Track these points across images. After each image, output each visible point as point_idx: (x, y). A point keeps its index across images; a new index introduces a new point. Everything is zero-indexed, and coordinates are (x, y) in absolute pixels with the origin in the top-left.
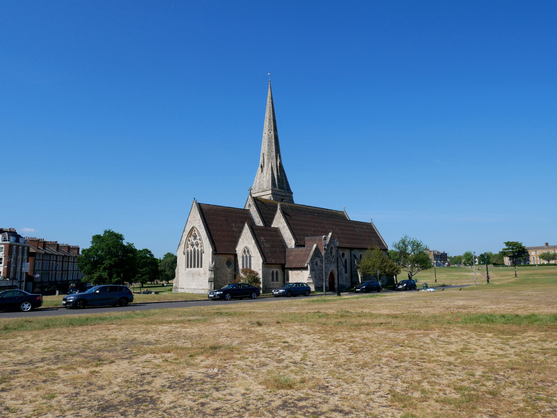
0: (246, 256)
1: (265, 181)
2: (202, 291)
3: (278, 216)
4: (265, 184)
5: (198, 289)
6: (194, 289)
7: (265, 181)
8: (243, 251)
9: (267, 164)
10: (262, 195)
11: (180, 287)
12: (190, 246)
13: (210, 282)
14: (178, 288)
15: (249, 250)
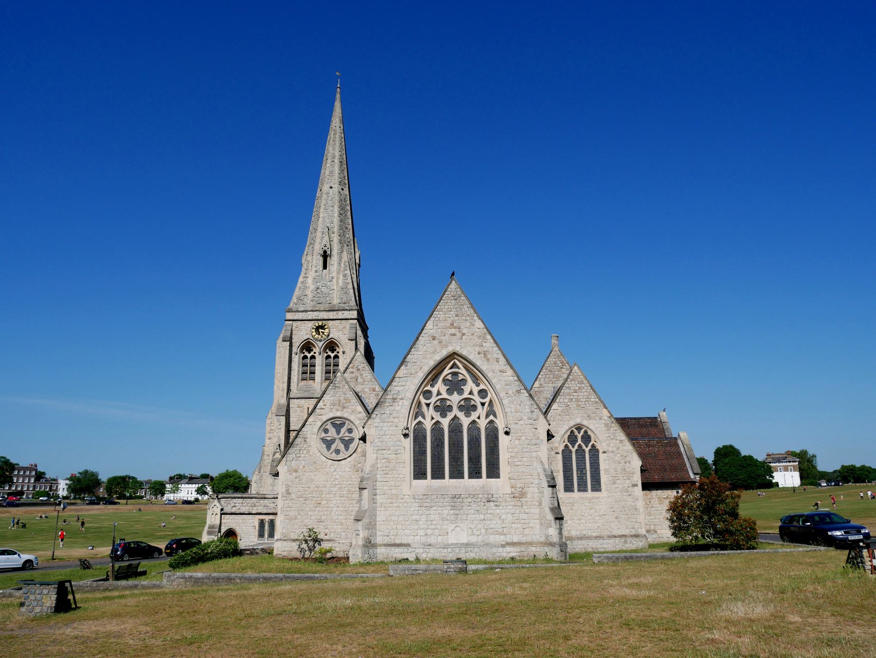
0: (580, 452)
1: (335, 287)
2: (508, 549)
4: (335, 295)
5: (487, 544)
6: (467, 545)
7: (335, 287)
8: (567, 436)
9: (338, 253)
10: (326, 318)
11: (379, 540)
12: (430, 412)
13: (558, 521)
14: (375, 546)
15: (590, 433)
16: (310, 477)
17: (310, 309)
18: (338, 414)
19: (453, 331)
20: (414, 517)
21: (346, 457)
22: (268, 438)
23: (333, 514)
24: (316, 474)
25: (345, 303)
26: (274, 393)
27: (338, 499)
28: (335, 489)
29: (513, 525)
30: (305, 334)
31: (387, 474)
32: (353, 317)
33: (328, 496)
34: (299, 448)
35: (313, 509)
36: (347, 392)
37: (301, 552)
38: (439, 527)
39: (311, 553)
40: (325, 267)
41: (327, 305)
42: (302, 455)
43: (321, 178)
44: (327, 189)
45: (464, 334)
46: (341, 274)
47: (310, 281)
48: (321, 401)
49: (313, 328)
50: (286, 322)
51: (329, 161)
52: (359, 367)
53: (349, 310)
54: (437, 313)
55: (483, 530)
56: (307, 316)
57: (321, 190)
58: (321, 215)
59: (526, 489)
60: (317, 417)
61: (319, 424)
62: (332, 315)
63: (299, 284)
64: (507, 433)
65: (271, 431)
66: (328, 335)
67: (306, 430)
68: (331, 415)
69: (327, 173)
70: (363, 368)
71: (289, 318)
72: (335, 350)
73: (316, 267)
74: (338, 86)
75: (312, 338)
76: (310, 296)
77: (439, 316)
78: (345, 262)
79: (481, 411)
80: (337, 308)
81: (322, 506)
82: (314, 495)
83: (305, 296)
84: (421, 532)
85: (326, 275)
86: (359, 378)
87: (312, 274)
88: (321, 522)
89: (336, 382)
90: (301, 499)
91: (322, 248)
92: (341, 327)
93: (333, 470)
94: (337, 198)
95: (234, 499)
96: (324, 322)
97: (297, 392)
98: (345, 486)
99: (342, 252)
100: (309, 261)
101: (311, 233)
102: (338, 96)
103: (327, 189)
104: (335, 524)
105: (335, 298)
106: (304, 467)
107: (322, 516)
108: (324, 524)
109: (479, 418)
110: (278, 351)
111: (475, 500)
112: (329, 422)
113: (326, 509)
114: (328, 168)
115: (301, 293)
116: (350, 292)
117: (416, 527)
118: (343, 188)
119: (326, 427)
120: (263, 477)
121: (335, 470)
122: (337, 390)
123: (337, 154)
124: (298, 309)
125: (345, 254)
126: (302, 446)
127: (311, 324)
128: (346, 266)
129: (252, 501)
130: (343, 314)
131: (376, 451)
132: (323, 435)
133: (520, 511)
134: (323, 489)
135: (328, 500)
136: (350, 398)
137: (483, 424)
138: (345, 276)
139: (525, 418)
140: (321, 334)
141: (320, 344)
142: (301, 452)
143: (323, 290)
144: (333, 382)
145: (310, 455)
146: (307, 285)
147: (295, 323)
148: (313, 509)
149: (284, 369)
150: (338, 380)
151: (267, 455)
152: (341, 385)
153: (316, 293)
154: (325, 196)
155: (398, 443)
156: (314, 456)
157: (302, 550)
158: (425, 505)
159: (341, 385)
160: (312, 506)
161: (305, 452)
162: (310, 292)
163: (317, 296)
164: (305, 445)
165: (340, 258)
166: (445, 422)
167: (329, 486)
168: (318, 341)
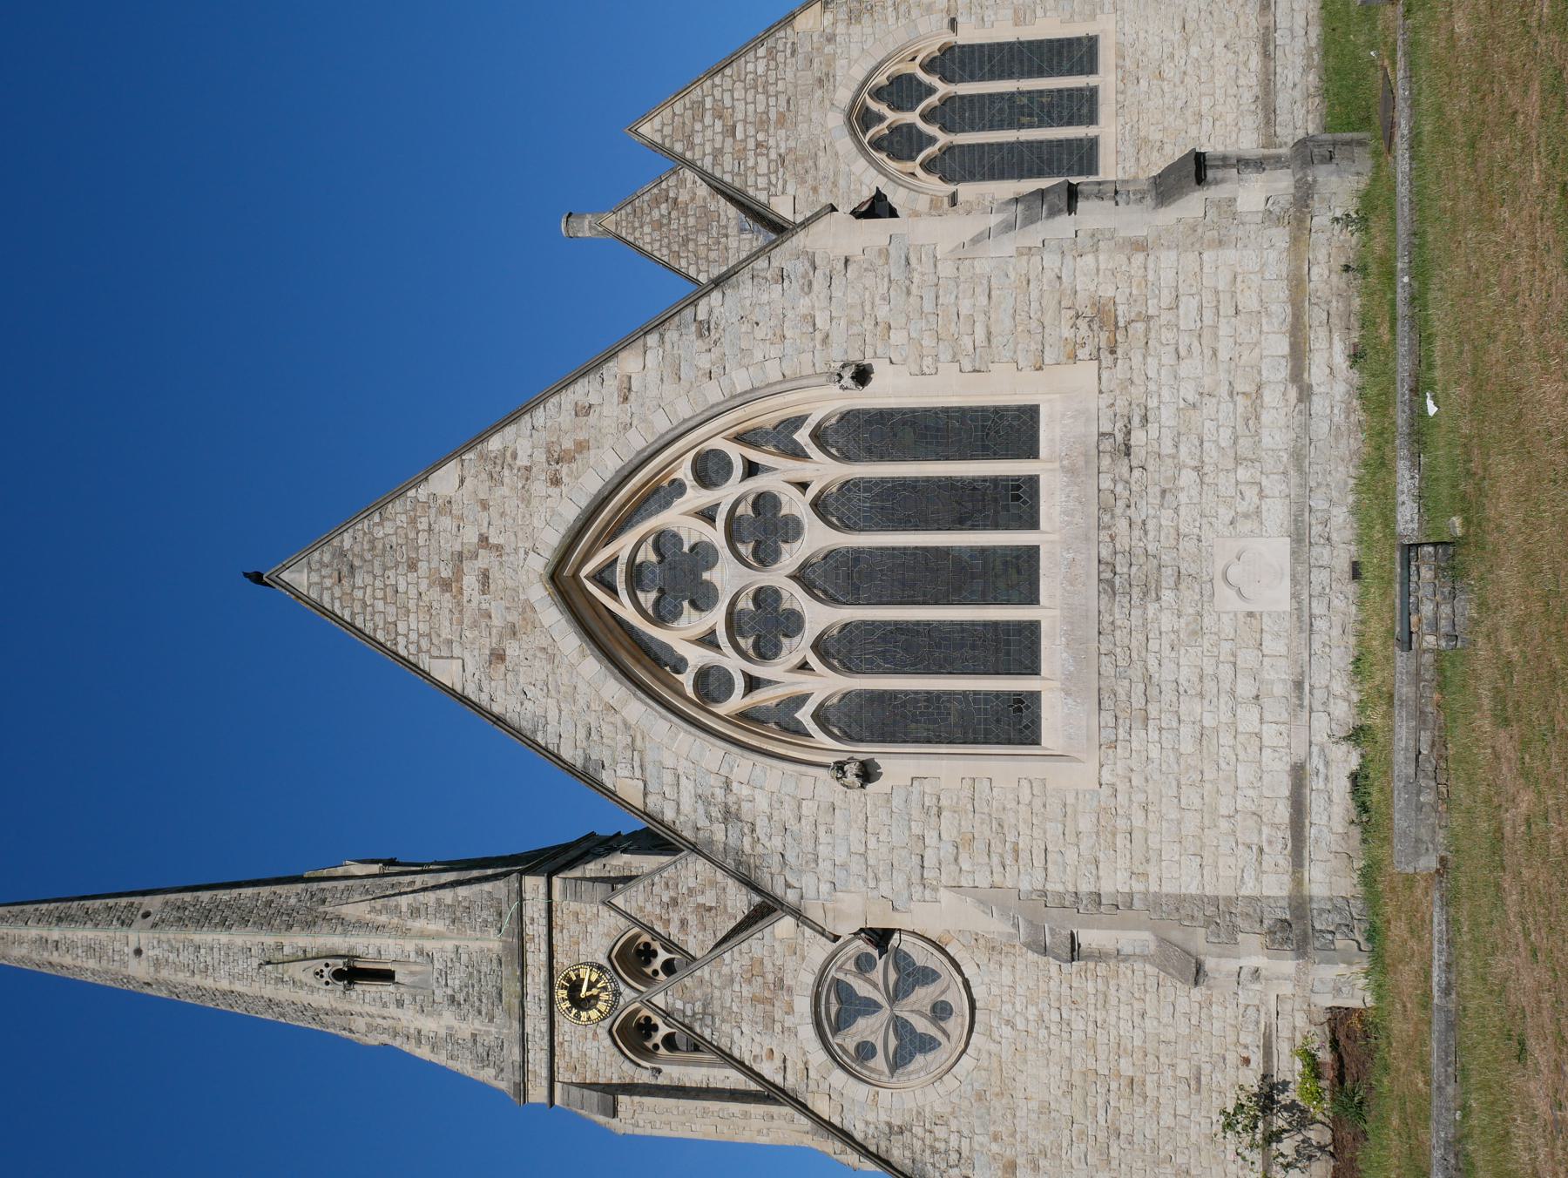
0: (951, 114)
2: (1316, 374)
3: (658, 225)
5: (1298, 457)
6: (1299, 538)
7: (449, 945)
8: (893, 166)
9: (345, 933)
10: (544, 974)
11: (1276, 886)
13: (1210, 174)
14: (1300, 904)
15: (881, 79)
16: (1034, 1116)
17: (516, 1025)
18: (803, 1005)
19: (470, 582)
20: (1187, 747)
21: (959, 979)
23: (1170, 1034)
24: (1020, 1094)
25: (500, 915)
26: (780, 1143)
27: (1113, 1013)
28: (1078, 1025)
29: (1223, 355)
30: (595, 1044)
31: (1016, 852)
32: (543, 890)
33: (1102, 1052)
34: (928, 1152)
35: (1150, 1106)
36: (726, 970)
37: (1310, 1158)
38: (1226, 647)
39: (1313, 1121)
40: (387, 976)
41: (506, 971)
42: (954, 1143)
43: (109, 983)
44: (144, 963)
45: (484, 539)
46: (410, 923)
47: (429, 1025)
48: (756, 1068)
49: (578, 1016)
50: (557, 1101)
51: (55, 957)
52: (666, 899)
53: (522, 900)
54: (401, 641)
55: (1243, 474)
56: (538, 1035)
57: (149, 984)
58: (224, 985)
59: (1082, 300)
60: (812, 1084)
61: (838, 1077)
62: (536, 957)
63: (441, 1059)
64: (862, 376)
66: (600, 968)
67: (860, 1126)
68: (808, 1032)
69: (92, 964)
70: (667, 885)
71: (545, 1092)
72: (647, 945)
73: (385, 1005)
75: (608, 1022)
76: (477, 1024)
77: (413, 636)
78: (373, 910)
79: (779, 475)
80: (516, 940)
81: (1139, 1074)
82: (1101, 1101)
83: (475, 1041)
84: (1248, 718)
85: (412, 973)
86: (701, 900)
87: (409, 1018)
88: (1199, 1080)
89: (689, 1013)
90: (1114, 1152)
91: (327, 983)
92: (574, 928)
93: (1006, 1031)
94: (171, 934)
96: (559, 980)
98: (1065, 985)
99: (341, 920)
100: (368, 1025)
101: (283, 1015)
103: (144, 963)
104: (1205, 1026)
105: (485, 945)
106: (996, 1138)
107: (1179, 1073)
108: (1206, 1068)
109: (803, 486)
110: (648, 1131)
111: (1121, 504)
112: (834, 1041)
113: (1150, 1058)
114: (79, 962)
115: (467, 1053)
116: (465, 898)
117: (1227, 739)
118: (141, 912)
119: (852, 1051)
121: (1008, 1022)
122: (716, 1007)
123: (33, 932)
124: (517, 1064)
125: (350, 911)
126: (918, 1144)
127: (565, 1025)
128: (385, 907)
130: (532, 919)
131: (927, 892)
132: (879, 1062)
133: (1169, 326)
134: (1078, 1065)
135: (1119, 1050)
136: (746, 961)
137: (825, 471)
138: (415, 912)
139: (804, 304)
140: (594, 991)
141: (627, 994)
142: (941, 1146)
143: (457, 982)
144: (687, 1021)
145: (953, 1113)
146: (443, 1033)
147: (562, 1075)
148: (1150, 1106)
149: (705, 1111)
150: (679, 1005)
152: (698, 993)
153: (466, 1007)
154: (165, 973)
155: (897, 802)
156: (955, 1100)
157: (1305, 1154)
158: (1137, 701)
159: (698, 993)
160: (1139, 1112)
161: (940, 1132)
162: (464, 1025)
163: (477, 1004)
164: (918, 1131)
165: (362, 925)
166: (820, 617)
167: (1066, 1045)
168: (616, 1001)
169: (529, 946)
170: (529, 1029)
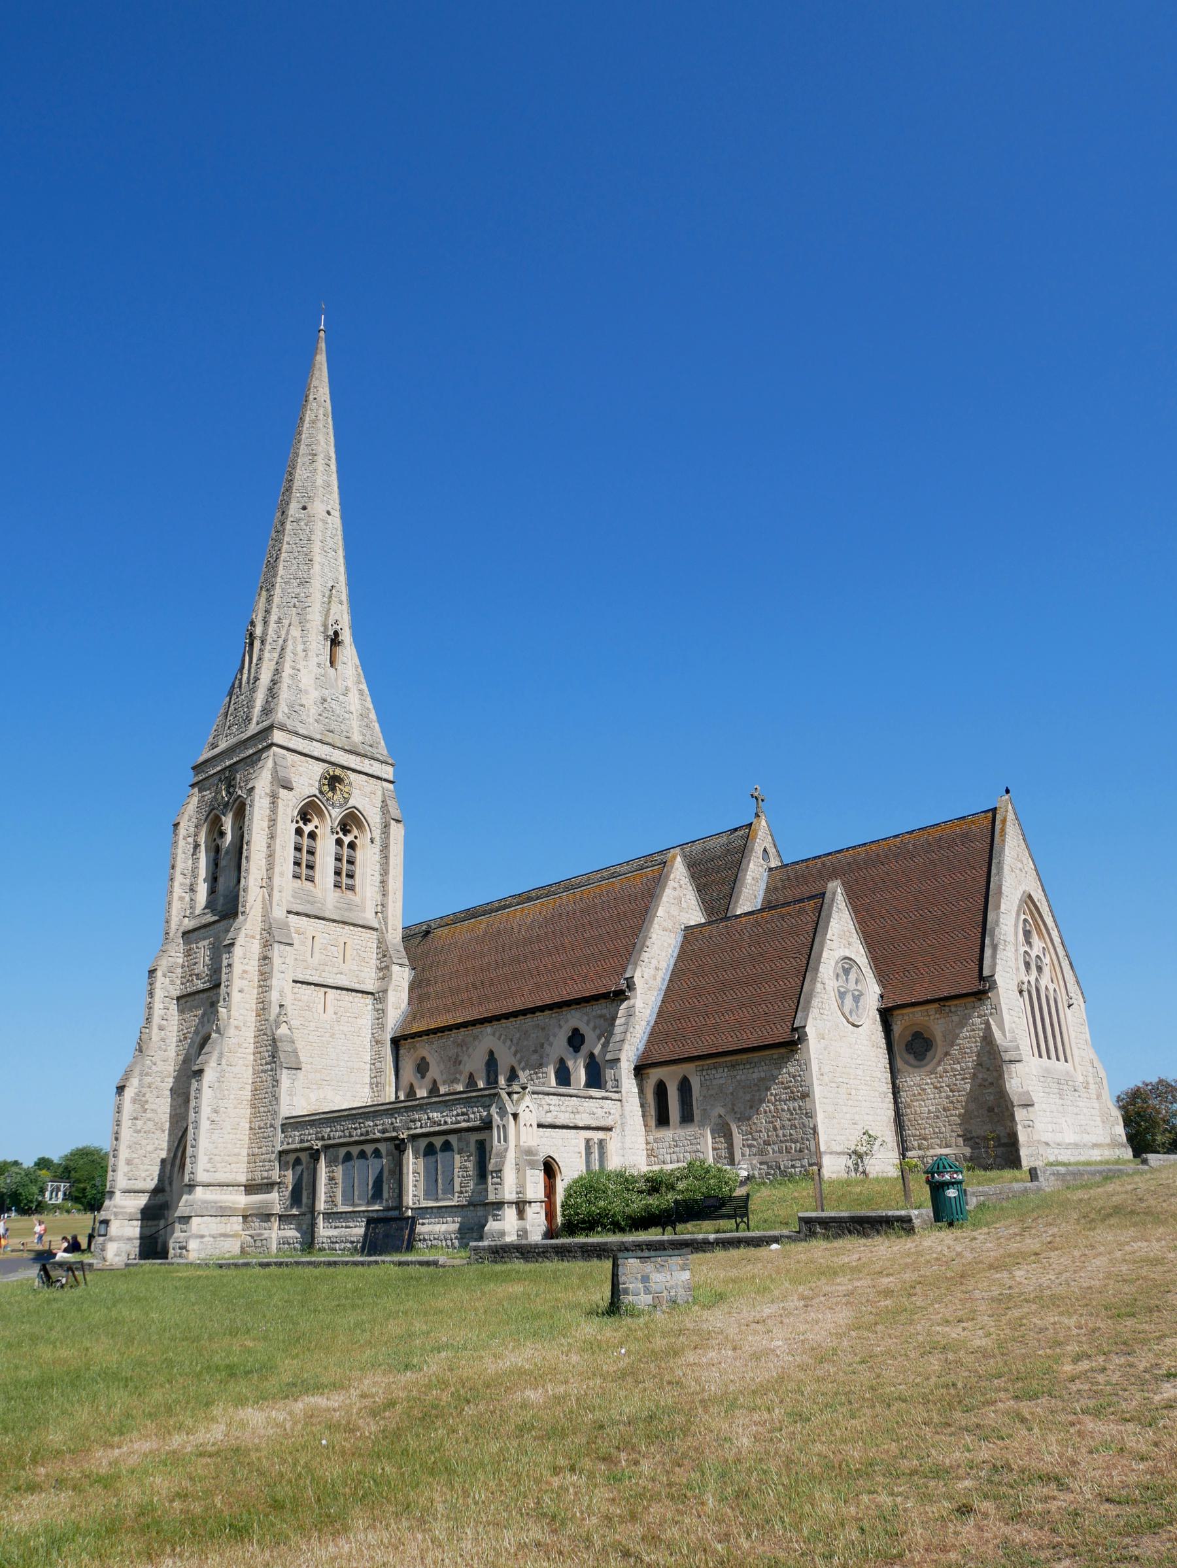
17: (318, 737)
22: (237, 990)
49: (326, 778)
53: (382, 762)
56: (312, 748)
58: (317, 558)
65: (245, 976)
71: (280, 742)
73: (317, 655)
74: (322, 327)
92: (368, 789)
95: (546, 1097)
97: (292, 900)
102: (322, 345)
120: (227, 1075)
129: (571, 1103)
151: (236, 1027)
162: (311, 702)
169: (358, 759)
170: (315, 743)
